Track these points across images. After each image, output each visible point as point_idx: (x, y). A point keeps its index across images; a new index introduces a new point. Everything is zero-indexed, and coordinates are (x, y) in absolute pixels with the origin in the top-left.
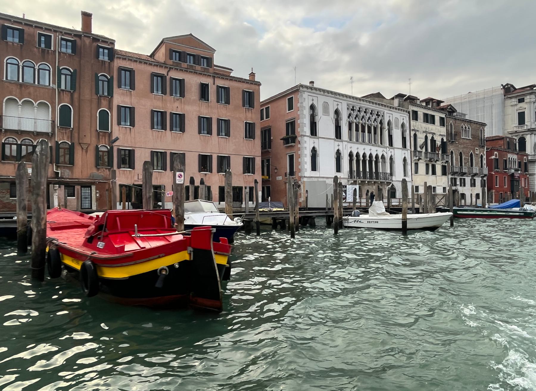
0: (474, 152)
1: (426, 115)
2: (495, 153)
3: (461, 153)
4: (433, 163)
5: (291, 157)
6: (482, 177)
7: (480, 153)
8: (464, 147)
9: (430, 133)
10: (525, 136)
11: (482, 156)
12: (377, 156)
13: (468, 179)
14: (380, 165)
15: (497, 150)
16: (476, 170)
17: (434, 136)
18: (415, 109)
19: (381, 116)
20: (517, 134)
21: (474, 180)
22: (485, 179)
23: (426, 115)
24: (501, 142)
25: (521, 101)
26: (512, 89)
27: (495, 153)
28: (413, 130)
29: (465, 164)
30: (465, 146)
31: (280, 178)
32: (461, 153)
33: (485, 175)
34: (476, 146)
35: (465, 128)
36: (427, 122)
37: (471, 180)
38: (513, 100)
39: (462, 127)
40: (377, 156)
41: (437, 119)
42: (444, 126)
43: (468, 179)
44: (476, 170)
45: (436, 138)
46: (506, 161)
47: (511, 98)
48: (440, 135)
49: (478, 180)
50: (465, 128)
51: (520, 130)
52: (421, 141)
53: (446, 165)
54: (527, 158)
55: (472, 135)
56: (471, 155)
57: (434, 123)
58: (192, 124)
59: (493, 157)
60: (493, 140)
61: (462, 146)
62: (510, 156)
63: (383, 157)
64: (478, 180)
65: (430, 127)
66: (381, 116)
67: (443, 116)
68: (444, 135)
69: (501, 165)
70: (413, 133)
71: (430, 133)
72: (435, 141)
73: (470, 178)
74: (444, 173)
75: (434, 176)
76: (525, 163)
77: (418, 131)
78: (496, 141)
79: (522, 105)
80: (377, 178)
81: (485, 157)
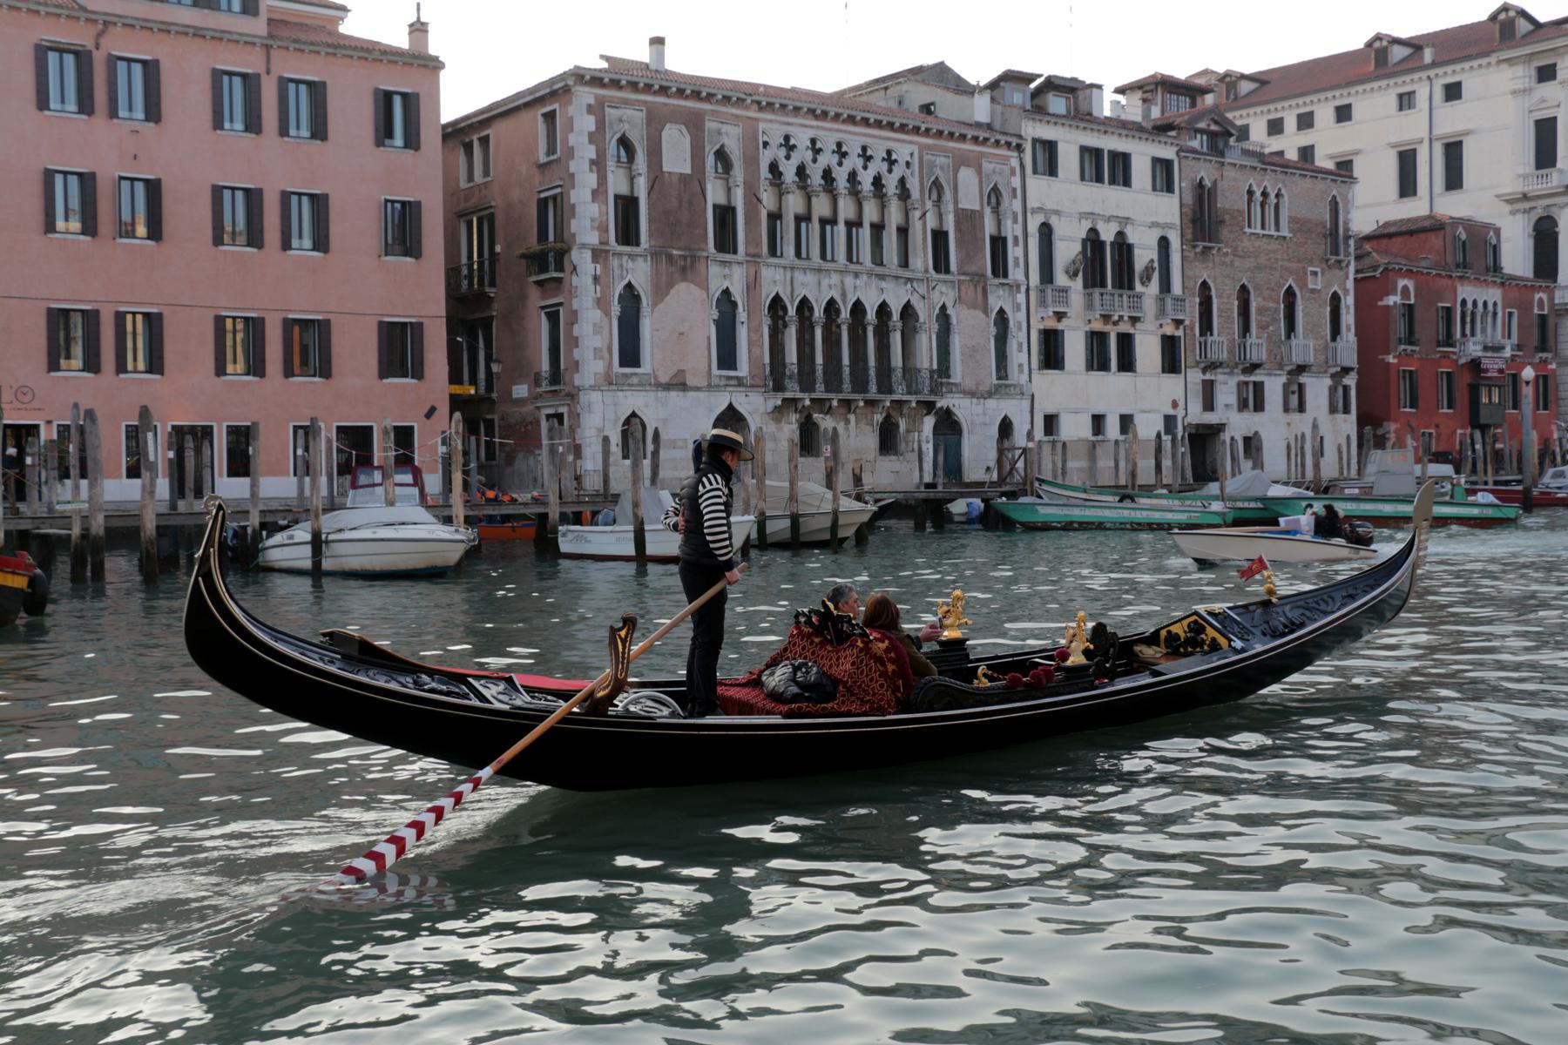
0: (1303, 286)
1: (1091, 155)
2: (1402, 283)
3: (1244, 290)
4: (1125, 328)
5: (553, 318)
6: (1333, 376)
7: (1328, 284)
8: (1258, 268)
9: (1109, 219)
10: (1555, 213)
11: (1335, 299)
12: (883, 310)
13: (1274, 387)
14: (896, 339)
15: (1410, 274)
16: (1304, 347)
17: (1129, 231)
18: (1046, 132)
19: (902, 162)
20: (1527, 205)
21: (1301, 387)
22: (1351, 381)
23: (1091, 155)
24: (1435, 241)
25: (1547, 74)
26: (1523, 26)
28: (1034, 211)
29: (1262, 327)
30: (1262, 260)
31: (521, 391)
32: (1244, 290)
33: (1346, 370)
34: (1311, 262)
37: (1286, 387)
38: (1519, 70)
40: (883, 310)
41: (1141, 170)
42: (1169, 188)
43: (1274, 387)
44: (1304, 347)
45: (1132, 237)
46: (1449, 312)
47: (1509, 61)
48: (1155, 225)
49: (1317, 389)
51: (1535, 188)
52: (1067, 250)
53: (1179, 333)
54: (1551, 299)
55: (1292, 220)
56: (1290, 293)
57: (1127, 183)
58: (188, 213)
59: (1392, 300)
60: (1411, 233)
61: (1250, 262)
62: (1467, 292)
63: (908, 311)
64: (1317, 389)
65: (1107, 199)
66: (902, 162)
67: (1168, 153)
68: (1170, 226)
69: (1427, 328)
70: (1034, 224)
71: (1109, 219)
72: (1130, 247)
73: (1283, 379)
74: (1171, 364)
75: (1126, 377)
76: (1543, 318)
77: (1058, 213)
78: (1422, 236)
79: (1549, 90)
80: (885, 386)
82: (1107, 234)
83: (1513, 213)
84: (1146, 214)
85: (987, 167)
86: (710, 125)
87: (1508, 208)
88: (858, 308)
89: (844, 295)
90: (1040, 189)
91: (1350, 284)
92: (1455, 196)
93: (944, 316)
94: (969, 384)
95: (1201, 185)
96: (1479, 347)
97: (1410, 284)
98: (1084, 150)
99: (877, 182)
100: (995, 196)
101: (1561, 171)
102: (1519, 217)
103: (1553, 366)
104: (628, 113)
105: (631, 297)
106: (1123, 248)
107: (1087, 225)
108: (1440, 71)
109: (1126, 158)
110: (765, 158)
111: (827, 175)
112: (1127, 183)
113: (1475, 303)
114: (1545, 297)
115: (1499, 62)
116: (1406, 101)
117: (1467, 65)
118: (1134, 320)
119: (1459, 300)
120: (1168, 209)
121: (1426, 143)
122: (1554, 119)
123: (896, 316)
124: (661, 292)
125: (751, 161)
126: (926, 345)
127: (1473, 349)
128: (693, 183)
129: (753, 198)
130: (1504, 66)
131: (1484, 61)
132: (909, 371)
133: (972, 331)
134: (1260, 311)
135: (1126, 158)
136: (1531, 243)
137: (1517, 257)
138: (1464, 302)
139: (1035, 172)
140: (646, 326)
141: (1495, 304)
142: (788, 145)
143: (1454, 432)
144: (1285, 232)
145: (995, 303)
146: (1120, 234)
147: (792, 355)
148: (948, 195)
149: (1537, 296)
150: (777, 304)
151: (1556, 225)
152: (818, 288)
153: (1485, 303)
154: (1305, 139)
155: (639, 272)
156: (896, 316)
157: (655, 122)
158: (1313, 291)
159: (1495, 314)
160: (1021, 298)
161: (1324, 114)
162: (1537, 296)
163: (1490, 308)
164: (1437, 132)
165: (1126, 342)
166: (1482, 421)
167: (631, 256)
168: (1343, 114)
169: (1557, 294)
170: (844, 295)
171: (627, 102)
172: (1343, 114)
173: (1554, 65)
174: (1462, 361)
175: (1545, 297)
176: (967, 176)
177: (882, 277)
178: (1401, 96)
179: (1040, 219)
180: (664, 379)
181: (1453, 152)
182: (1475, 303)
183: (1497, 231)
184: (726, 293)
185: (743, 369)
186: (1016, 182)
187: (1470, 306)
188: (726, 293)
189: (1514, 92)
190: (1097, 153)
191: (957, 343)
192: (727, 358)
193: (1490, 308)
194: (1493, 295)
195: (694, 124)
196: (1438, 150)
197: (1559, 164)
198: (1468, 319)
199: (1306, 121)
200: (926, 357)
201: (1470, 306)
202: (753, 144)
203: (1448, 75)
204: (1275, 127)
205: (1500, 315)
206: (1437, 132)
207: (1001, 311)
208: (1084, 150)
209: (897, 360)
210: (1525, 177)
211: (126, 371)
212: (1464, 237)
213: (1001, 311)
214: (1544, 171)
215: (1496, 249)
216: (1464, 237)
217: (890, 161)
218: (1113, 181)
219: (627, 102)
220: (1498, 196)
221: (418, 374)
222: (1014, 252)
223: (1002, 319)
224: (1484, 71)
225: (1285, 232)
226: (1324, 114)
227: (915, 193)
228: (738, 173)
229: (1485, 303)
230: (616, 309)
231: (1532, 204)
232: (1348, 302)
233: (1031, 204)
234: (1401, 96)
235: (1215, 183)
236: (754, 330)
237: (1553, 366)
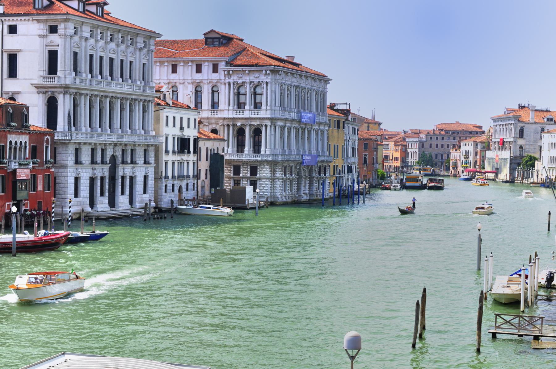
10: (56, 95)
20: (44, 90)
25: (53, 30)
38: (42, 26)
47: (38, 21)
51: (49, 83)
54: (52, 138)
62: (13, 138)
79: (53, 37)
83: (38, 93)
87: (36, 90)
92: (12, 81)
96: (17, 164)
101: (59, 77)
102: (41, 95)
103: (53, 170)
108: (7, 18)
113: (16, 142)
114: (49, 138)
115: (33, 20)
117: (19, 18)
119: (8, 141)
122: (57, 51)
127: (14, 165)
130: (35, 22)
131: (27, 18)
136: (46, 107)
137: (37, 119)
138: (11, 142)
141: (26, 142)
143: (5, 203)
149: (46, 138)
151: (57, 102)
153: (21, 142)
159: (26, 147)
162: (46, 138)
163: (23, 144)
166: (18, 199)
169: (56, 135)
173: (57, 26)
174: (9, 171)
175: (49, 138)
182: (16, 142)
183: (28, 108)
187: (13, 144)
189: (39, 36)
193: (23, 144)
194: (24, 139)
197: (58, 74)
198: (13, 151)
201: (13, 144)
205: (28, 147)
206: (5, 48)
210: (44, 77)
212: (11, 111)
214: (52, 76)
215: (27, 118)
216: (11, 111)
220: (32, 84)
224: (26, 22)
229: (21, 142)
231: (47, 90)
237: (53, 170)
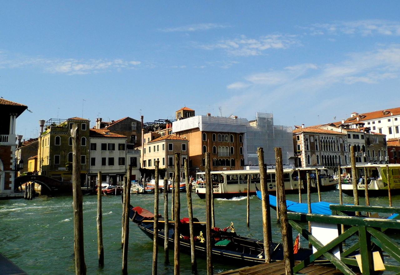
1: (354, 135)
2: (393, 148)
4: (360, 157)
7: (384, 149)
11: (385, 151)
12: (333, 156)
14: (335, 159)
17: (359, 144)
23: (354, 135)
27: (393, 148)
32: (373, 151)
34: (382, 147)
35: (375, 138)
36: (355, 138)
39: (373, 138)
40: (333, 156)
41: (360, 137)
42: (363, 139)
50: (375, 138)
55: (379, 141)
57: (358, 138)
60: (393, 141)
63: (336, 156)
65: (356, 140)
72: (359, 146)
77: (351, 143)
80: (334, 166)
81: (387, 151)
82: (357, 145)
84: (361, 142)
85: (343, 138)
86: (315, 136)
88: (331, 156)
89: (329, 155)
90: (349, 140)
91: (387, 149)
93: (339, 157)
94: (343, 164)
95: (367, 138)
97: (394, 148)
98: (353, 135)
99: (326, 140)
100: (344, 142)
104: (307, 136)
105: (309, 156)
106: (359, 147)
107: (354, 144)
109: (358, 135)
110: (320, 139)
111: (326, 140)
112: (358, 138)
116: (389, 120)
118: (361, 156)
120: (363, 141)
121: (393, 126)
123: (334, 157)
124: (311, 155)
125: (319, 139)
126: (338, 160)
128: (314, 143)
129: (319, 144)
132: (336, 163)
133: (342, 158)
134: (376, 153)
135: (358, 135)
139: (348, 138)
140: (310, 159)
142: (322, 138)
144: (378, 143)
145: (345, 154)
146: (358, 145)
147: (324, 162)
148: (339, 142)
150: (323, 156)
152: (326, 154)
154: (374, 125)
155: (309, 154)
156: (334, 157)
157: (310, 136)
158: (382, 150)
160: (348, 154)
161: (376, 122)
164: (394, 125)
165: (360, 158)
167: (309, 152)
168: (380, 122)
170: (329, 155)
171: (307, 134)
172: (380, 122)
176: (341, 139)
177: (333, 152)
178: (388, 120)
179: (349, 144)
180: (312, 165)
181: (397, 127)
184: (318, 155)
185: (320, 164)
186: (346, 139)
188: (318, 155)
190: (355, 135)
191: (341, 159)
192: (318, 163)
195: (313, 136)
196: (395, 128)
199: (374, 123)
200: (338, 162)
202: (319, 137)
203: (396, 117)
204: (369, 123)
207: (346, 156)
208: (353, 135)
209: (335, 162)
211: (214, 165)
213: (346, 156)
217: (332, 138)
218: (357, 138)
219: (307, 134)
221: (306, 167)
222: (346, 148)
223: (346, 156)
225: (378, 143)
226: (376, 122)
227: (335, 142)
228: (318, 141)
230: (307, 158)
232: (387, 151)
233: (348, 142)
234: (388, 120)
235: (369, 138)
236: (320, 159)
